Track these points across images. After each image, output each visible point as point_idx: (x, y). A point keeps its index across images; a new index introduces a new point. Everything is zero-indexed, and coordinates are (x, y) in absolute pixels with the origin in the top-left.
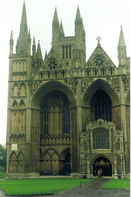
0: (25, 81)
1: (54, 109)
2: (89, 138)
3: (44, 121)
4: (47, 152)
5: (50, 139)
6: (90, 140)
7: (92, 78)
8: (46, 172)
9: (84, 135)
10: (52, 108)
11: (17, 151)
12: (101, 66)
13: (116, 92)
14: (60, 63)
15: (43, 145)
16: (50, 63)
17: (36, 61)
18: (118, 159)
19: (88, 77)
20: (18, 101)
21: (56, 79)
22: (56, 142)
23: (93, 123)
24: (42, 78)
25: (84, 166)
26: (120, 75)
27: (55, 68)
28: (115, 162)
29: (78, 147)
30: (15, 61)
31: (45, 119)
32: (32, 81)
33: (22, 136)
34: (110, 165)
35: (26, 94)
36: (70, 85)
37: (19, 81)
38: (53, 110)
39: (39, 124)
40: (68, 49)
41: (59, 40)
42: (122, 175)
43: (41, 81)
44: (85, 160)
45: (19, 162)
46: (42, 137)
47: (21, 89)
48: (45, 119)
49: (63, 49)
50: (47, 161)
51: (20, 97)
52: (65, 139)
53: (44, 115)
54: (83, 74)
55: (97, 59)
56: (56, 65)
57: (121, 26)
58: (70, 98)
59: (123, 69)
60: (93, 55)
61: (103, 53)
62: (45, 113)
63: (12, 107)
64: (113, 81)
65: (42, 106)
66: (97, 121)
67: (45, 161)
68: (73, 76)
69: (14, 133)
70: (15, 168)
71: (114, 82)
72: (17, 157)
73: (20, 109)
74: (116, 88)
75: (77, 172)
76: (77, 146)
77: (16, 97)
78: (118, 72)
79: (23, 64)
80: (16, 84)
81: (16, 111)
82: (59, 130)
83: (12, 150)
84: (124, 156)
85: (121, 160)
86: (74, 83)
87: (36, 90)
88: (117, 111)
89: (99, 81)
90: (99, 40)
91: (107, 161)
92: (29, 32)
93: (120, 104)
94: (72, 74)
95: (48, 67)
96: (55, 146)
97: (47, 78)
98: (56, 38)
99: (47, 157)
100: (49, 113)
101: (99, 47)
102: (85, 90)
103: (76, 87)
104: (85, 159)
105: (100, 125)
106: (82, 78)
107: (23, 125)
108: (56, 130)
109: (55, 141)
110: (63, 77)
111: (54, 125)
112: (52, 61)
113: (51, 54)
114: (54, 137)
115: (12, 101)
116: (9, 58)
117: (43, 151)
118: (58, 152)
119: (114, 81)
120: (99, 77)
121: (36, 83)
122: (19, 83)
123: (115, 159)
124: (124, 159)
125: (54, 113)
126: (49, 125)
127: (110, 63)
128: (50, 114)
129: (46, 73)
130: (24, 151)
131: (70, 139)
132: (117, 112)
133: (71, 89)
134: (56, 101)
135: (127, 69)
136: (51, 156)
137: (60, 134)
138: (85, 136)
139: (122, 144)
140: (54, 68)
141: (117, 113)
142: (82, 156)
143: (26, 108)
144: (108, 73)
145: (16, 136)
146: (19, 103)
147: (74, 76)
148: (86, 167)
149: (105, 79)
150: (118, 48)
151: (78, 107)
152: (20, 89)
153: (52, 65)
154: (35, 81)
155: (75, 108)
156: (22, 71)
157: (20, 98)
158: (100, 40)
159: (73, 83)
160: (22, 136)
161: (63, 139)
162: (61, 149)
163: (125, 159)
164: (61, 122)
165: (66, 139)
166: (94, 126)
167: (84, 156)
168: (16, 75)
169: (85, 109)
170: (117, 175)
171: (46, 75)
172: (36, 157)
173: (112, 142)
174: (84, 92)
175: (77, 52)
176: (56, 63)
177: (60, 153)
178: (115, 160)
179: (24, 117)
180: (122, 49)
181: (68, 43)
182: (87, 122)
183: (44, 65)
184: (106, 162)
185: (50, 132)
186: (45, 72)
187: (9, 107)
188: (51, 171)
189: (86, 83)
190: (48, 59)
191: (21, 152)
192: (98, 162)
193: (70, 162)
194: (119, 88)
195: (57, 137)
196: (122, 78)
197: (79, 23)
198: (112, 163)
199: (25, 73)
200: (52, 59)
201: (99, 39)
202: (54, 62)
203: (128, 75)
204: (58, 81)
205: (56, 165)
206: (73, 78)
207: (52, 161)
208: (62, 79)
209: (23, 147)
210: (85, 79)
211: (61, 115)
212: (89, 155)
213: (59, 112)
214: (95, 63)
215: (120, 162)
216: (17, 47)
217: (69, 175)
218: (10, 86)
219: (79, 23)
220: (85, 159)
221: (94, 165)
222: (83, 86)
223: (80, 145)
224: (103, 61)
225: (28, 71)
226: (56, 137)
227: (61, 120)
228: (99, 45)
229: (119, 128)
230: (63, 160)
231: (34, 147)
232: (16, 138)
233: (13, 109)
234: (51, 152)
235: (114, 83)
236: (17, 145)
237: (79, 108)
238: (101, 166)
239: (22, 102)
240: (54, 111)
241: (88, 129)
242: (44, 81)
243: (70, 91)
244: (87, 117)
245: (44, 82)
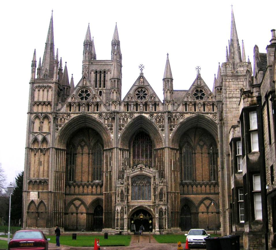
0: (50, 113)
1: (82, 150)
2: (128, 187)
3: (69, 164)
4: (72, 202)
5: (76, 187)
6: (128, 189)
7: (132, 113)
8: (71, 227)
9: (121, 183)
10: (79, 148)
11: (37, 200)
12: (144, 101)
13: (160, 132)
14: (94, 93)
15: (68, 195)
16: (81, 92)
17: (63, 89)
18: (161, 212)
19: (127, 113)
20: (40, 138)
21: (89, 113)
22: (84, 190)
23: (133, 168)
24: (70, 111)
25: (120, 220)
26: (165, 112)
27: (88, 98)
28: (157, 216)
29: (113, 198)
30: (37, 88)
31: (71, 162)
32: (57, 113)
33: (44, 183)
34: (151, 219)
35: (49, 129)
36: (105, 121)
37: (41, 113)
38: (81, 150)
39: (64, 168)
40: (102, 75)
41: (92, 63)
42: (164, 229)
43: (69, 115)
44: (122, 213)
45: (40, 215)
46: (67, 185)
47: (44, 123)
48: (71, 162)
49: (96, 75)
50: (72, 214)
51: (42, 133)
52: (94, 187)
53: (69, 156)
54: (122, 108)
55: (138, 91)
56: (89, 95)
57: (168, 55)
58: (104, 137)
59: (169, 104)
60: (134, 85)
61: (146, 84)
62: (71, 155)
63: (31, 145)
64: (157, 118)
65: (68, 146)
66: (137, 167)
67: (69, 214)
68: (109, 110)
69: (34, 178)
70: (34, 221)
71: (158, 119)
72: (38, 208)
73: (41, 148)
74: (160, 127)
75: (112, 228)
76: (112, 196)
77: (37, 133)
78: (163, 108)
79: (48, 91)
80: (37, 117)
81: (37, 150)
82: (87, 176)
83: (30, 199)
84: (167, 209)
85: (164, 213)
86: (110, 119)
87: (63, 125)
88: (161, 154)
89: (141, 118)
90: (142, 68)
91: (147, 215)
92: (57, 51)
93: (164, 146)
94: (108, 108)
95: (78, 96)
97: (77, 111)
98: (88, 61)
99: (72, 208)
100: (76, 154)
101: (141, 76)
102: (123, 128)
103: (112, 123)
104: (121, 212)
105: (141, 171)
106: (121, 113)
107: (45, 168)
108: (84, 176)
109: (82, 189)
110: (97, 110)
111: (82, 169)
112: (84, 90)
113: (84, 81)
114: (81, 184)
115: (32, 138)
116: (30, 83)
117: (67, 202)
118: (86, 203)
119: (158, 118)
120: (140, 113)
121: (63, 117)
122: (41, 115)
123: (157, 212)
124: (167, 212)
125: (82, 154)
126: (75, 169)
127: (154, 96)
128: (77, 155)
129: (76, 105)
130: (45, 200)
131: (101, 186)
132: (161, 156)
133: (106, 126)
134: (85, 139)
135: (173, 105)
136: (77, 208)
137: (88, 181)
138: (122, 184)
139: (165, 194)
140: (86, 98)
141: (160, 158)
142: (119, 208)
143: (49, 147)
144: (151, 108)
145: (36, 182)
146: (40, 141)
147: (110, 110)
148: (123, 221)
149: (147, 116)
150: (163, 79)
151: (114, 148)
152: (43, 123)
153: (84, 95)
154: (62, 113)
155: (111, 149)
156: (45, 100)
157: (42, 134)
158: (143, 68)
159: (108, 118)
160: (44, 183)
161: (92, 187)
162: (89, 199)
163: (168, 212)
164: (90, 166)
165: (97, 187)
166: (134, 172)
167: (121, 208)
168: (38, 105)
169: (122, 151)
170: (158, 230)
171: (76, 107)
172: (61, 209)
173: (155, 192)
174: (122, 131)
175: (115, 81)
176: (89, 92)
177: (89, 204)
178: (157, 213)
179: (46, 158)
180: (168, 81)
181: (103, 68)
182: (125, 167)
183: (73, 95)
184: (146, 216)
185: (76, 179)
186: (75, 103)
187: (27, 145)
188: (77, 226)
189: (126, 119)
190: (79, 87)
191: (42, 202)
192: (137, 216)
193: (103, 216)
194: (163, 127)
195: (85, 184)
196: (168, 115)
197: (116, 44)
198: (153, 217)
199: (49, 103)
200: (83, 87)
201: (142, 67)
202: (86, 91)
203: (174, 113)
204: (91, 115)
205: (83, 217)
206: (110, 113)
207: (79, 214)
208: (95, 113)
209: (44, 196)
210: (123, 114)
211: (91, 157)
212: (126, 206)
213: (89, 154)
214: (136, 96)
215: (163, 215)
216: (39, 69)
217: (101, 231)
218: (30, 119)
219: (116, 44)
220: (121, 212)
221: (132, 219)
222: (122, 123)
223: (116, 194)
224: (146, 94)
225: (53, 101)
226: (83, 184)
227: (90, 162)
228: (142, 74)
229: (162, 175)
230: (92, 212)
231: (58, 196)
232: (36, 185)
233: (32, 148)
234: (77, 203)
235: (158, 121)
236: (36, 193)
237: (115, 149)
238: (140, 220)
239: (44, 140)
240: (82, 151)
241: (126, 176)
242: (73, 115)
243: (105, 129)
244: (124, 161)
245: (73, 116)
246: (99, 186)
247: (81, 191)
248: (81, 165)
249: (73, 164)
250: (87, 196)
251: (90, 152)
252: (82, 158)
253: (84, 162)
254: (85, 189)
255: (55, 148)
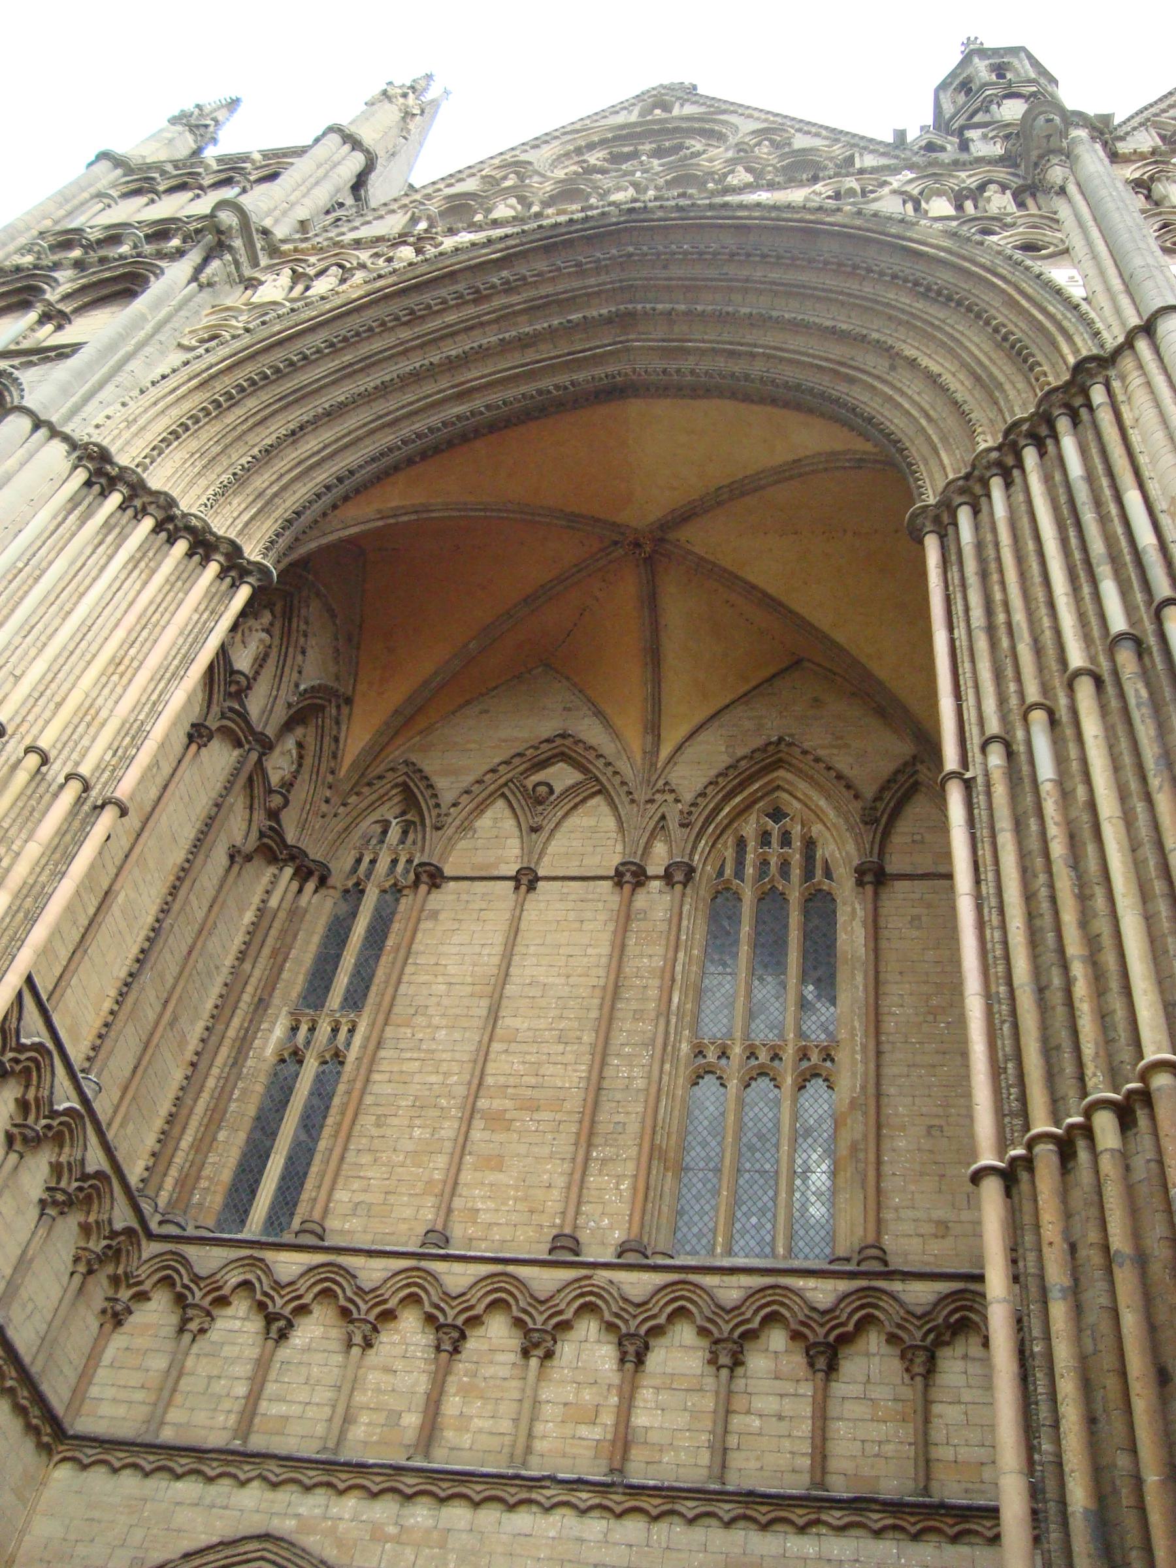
22: (452, 1405)
82: (556, 1173)
96: (384, 1511)
108: (496, 1163)
111: (483, 1056)
125: (527, 880)
126: (371, 1063)
151: (1148, 329)
164: (633, 1031)
195: (502, 1293)
246: (777, 1339)
247: (394, 1417)
248: (481, 1008)
249: (355, 1000)
250: (489, 1516)
251: (655, 867)
252: (514, 930)
253: (525, 970)
254: (466, 1391)
255: (66, 438)
